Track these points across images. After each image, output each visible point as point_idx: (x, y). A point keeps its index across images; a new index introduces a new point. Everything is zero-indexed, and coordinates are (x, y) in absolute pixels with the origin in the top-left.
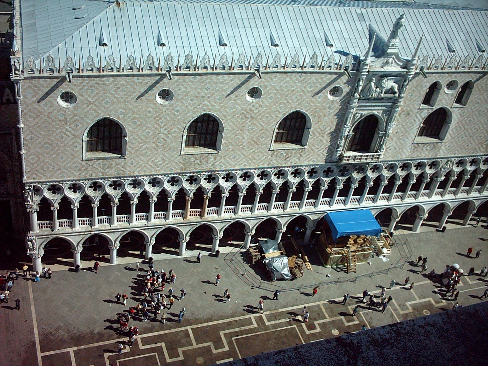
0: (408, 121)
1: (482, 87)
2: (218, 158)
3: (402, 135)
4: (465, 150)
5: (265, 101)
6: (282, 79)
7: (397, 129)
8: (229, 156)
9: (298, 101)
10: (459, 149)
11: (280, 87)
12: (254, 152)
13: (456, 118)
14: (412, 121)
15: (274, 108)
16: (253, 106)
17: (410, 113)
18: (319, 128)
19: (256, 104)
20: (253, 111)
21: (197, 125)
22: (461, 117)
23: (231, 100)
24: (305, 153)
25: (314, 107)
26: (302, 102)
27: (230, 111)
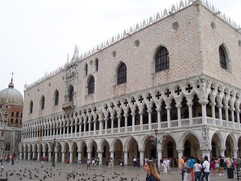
1: (101, 59)
22: (97, 76)
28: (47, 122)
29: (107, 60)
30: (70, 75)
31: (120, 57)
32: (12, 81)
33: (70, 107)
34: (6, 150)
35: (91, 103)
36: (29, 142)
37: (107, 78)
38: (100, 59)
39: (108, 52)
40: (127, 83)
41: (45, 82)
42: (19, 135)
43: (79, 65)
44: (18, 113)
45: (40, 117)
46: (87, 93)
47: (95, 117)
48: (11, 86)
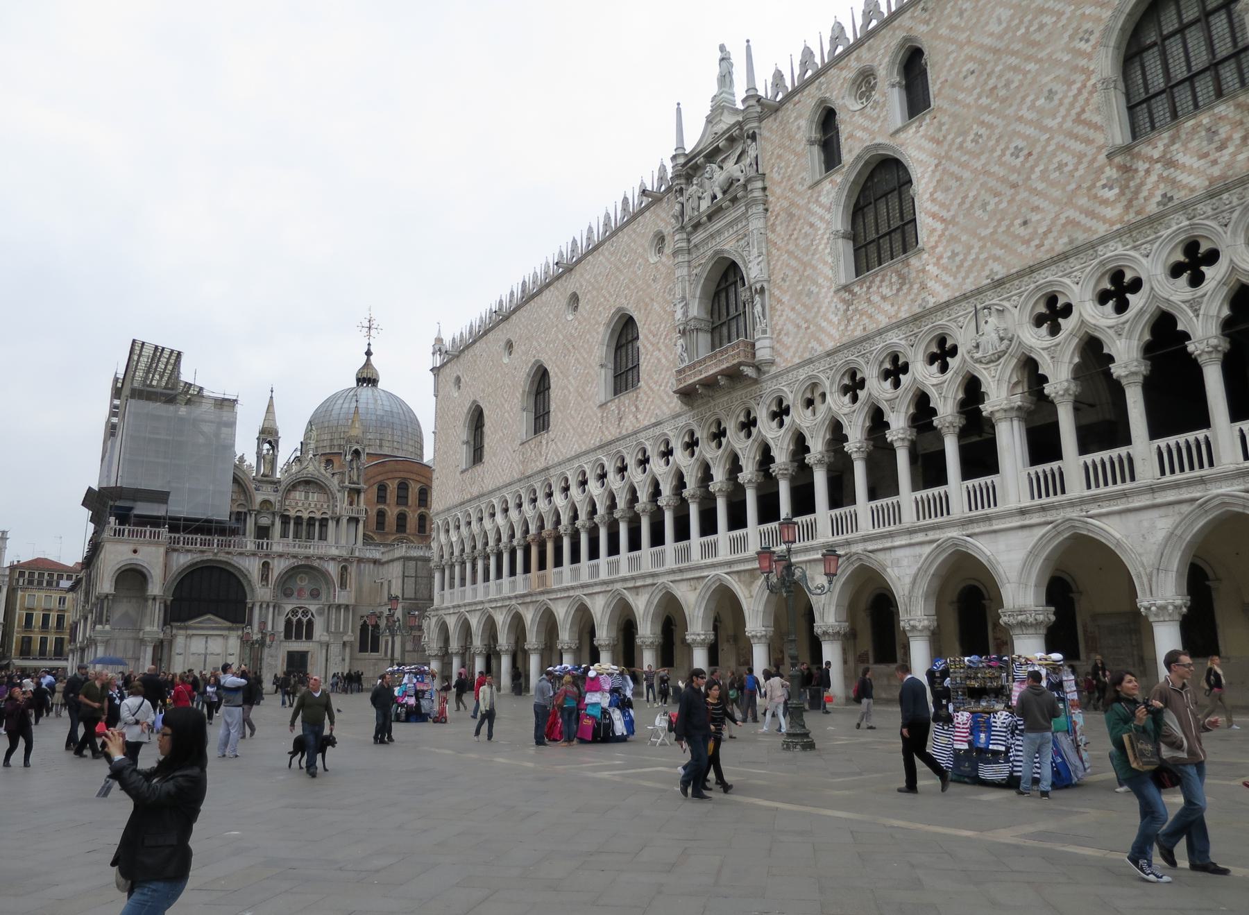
1: (953, 28)
7: (781, 269)
10: (999, 252)
13: (923, 157)
14: (806, 228)
17: (794, 211)
18: (651, 332)
28: (575, 491)
30: (705, 205)
32: (368, 360)
33: (734, 375)
34: (363, 648)
35: (904, 314)
36: (475, 603)
37: (1030, 123)
38: (943, 31)
41: (547, 295)
42: (421, 574)
43: (769, 130)
44: (403, 487)
45: (529, 472)
46: (845, 273)
47: (951, 395)
48: (367, 379)
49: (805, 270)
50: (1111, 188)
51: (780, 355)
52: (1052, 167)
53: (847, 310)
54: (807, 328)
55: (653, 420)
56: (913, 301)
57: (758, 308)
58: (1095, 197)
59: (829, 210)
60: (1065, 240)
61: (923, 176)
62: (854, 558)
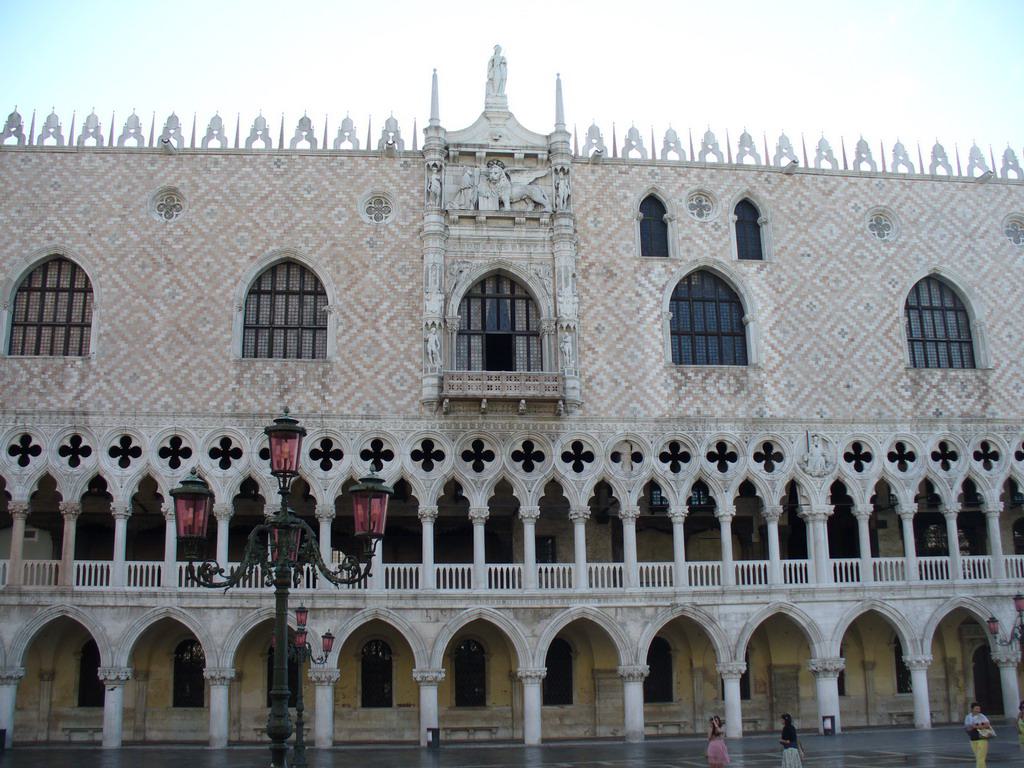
0: (616, 293)
1: (792, 211)
2: (92, 377)
3: (620, 339)
4: (850, 401)
5: (197, 221)
6: (233, 169)
7: (594, 318)
8: (120, 374)
9: (283, 223)
10: (826, 397)
11: (232, 188)
12: (185, 364)
15: (224, 240)
16: (170, 233)
19: (176, 227)
20: (170, 246)
21: (43, 298)
23: (111, 216)
24: (335, 379)
25: (329, 243)
26: (293, 227)
27: (113, 242)
29: (837, 231)
31: (930, 248)
35: (741, 413)
39: (838, 193)
40: (994, 376)
49: (627, 332)
50: (907, 391)
51: (590, 402)
52: (869, 357)
53: (679, 388)
54: (627, 388)
55: (360, 411)
56: (751, 407)
57: (568, 347)
58: (897, 391)
59: (662, 290)
60: (876, 410)
61: (763, 310)
62: (679, 609)
